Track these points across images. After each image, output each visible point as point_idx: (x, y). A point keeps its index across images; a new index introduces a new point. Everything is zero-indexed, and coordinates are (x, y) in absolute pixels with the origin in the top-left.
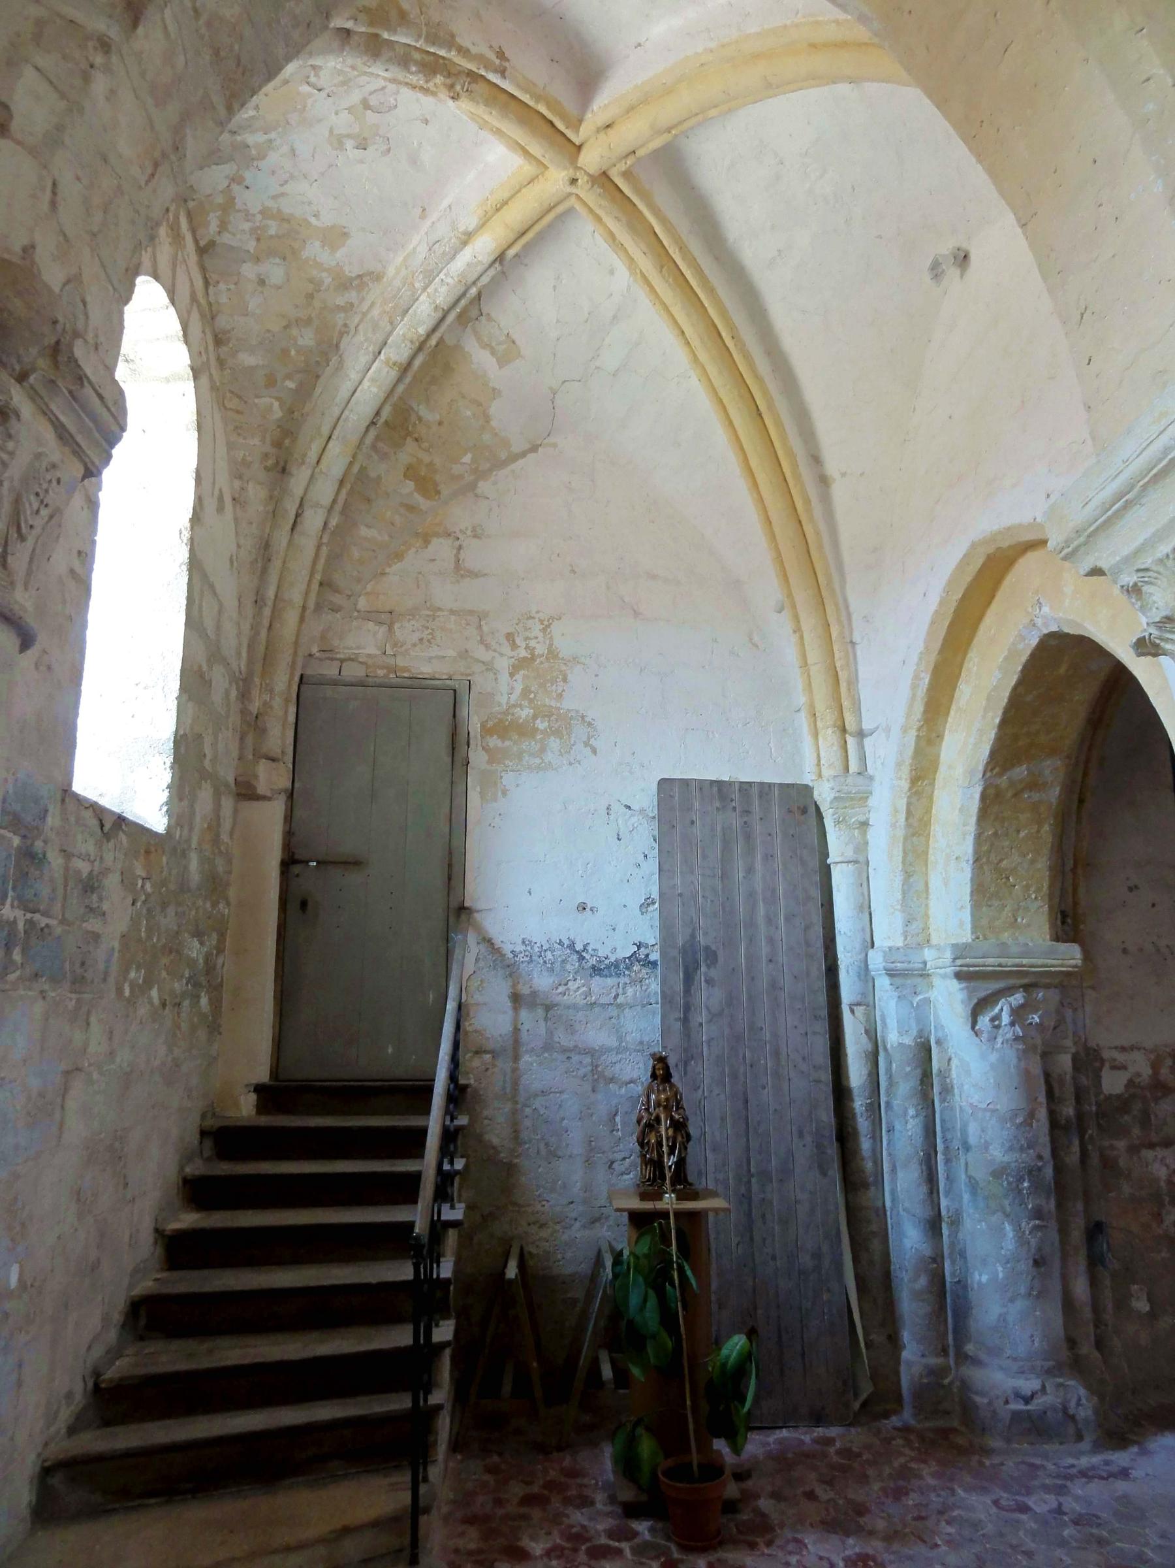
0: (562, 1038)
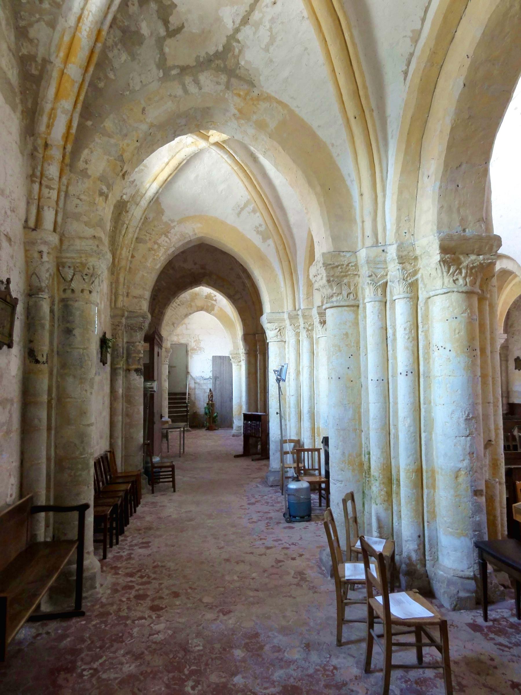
0: (201, 388)
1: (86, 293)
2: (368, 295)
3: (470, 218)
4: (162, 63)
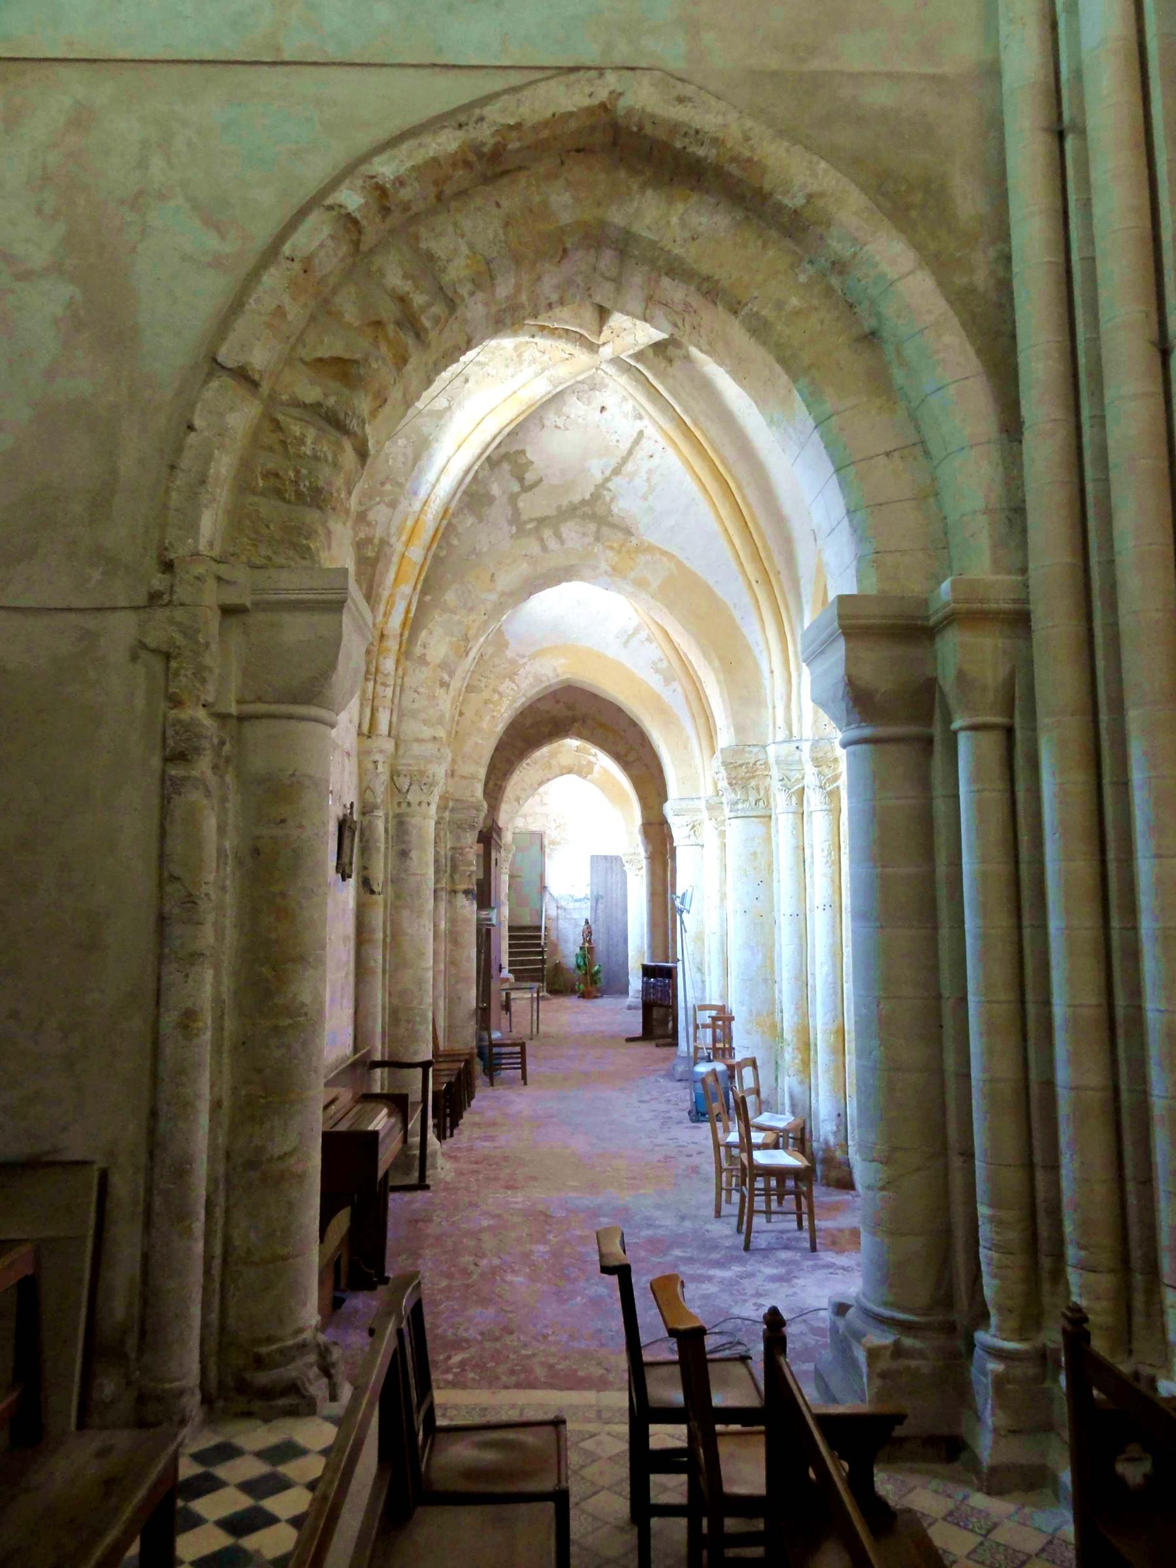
1: (424, 805)
2: (781, 802)
4: (516, 519)
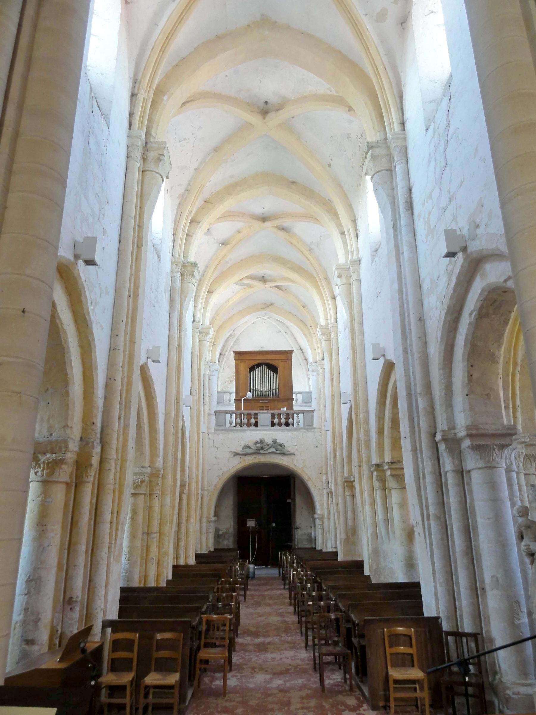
3: (56, 426)
